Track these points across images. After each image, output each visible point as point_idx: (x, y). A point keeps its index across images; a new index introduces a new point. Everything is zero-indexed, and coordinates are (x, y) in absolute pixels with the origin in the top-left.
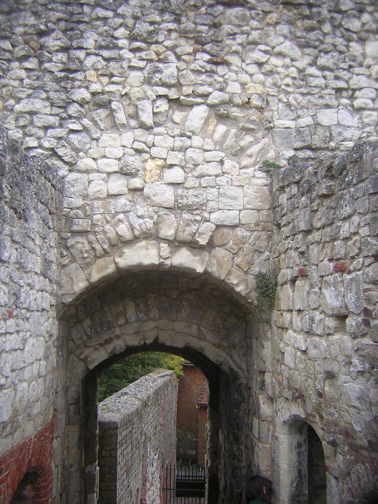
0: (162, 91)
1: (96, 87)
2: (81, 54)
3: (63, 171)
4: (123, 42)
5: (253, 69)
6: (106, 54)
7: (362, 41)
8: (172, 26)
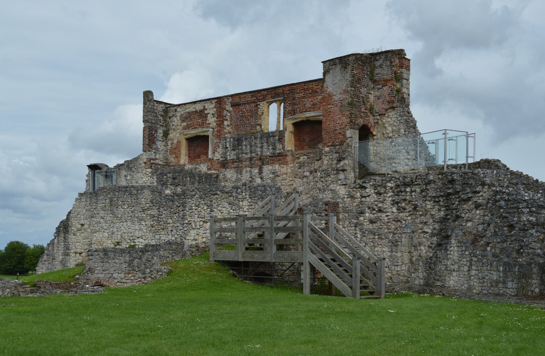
0: (201, 219)
1: (189, 219)
2: (186, 211)
3: (184, 240)
4: (194, 208)
5: (219, 212)
6: (190, 211)
7: (242, 201)
8: (203, 202)
